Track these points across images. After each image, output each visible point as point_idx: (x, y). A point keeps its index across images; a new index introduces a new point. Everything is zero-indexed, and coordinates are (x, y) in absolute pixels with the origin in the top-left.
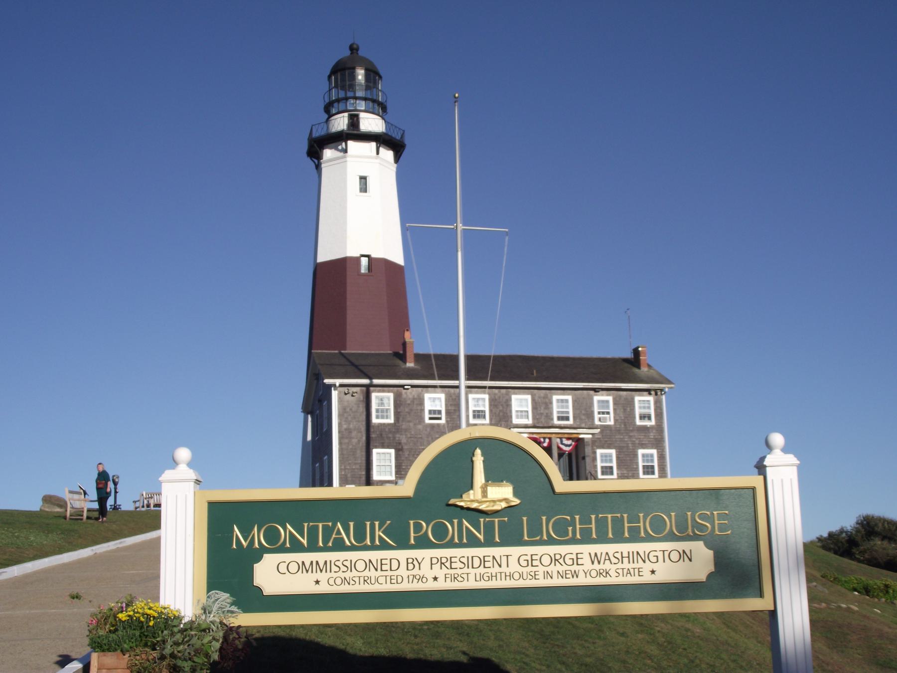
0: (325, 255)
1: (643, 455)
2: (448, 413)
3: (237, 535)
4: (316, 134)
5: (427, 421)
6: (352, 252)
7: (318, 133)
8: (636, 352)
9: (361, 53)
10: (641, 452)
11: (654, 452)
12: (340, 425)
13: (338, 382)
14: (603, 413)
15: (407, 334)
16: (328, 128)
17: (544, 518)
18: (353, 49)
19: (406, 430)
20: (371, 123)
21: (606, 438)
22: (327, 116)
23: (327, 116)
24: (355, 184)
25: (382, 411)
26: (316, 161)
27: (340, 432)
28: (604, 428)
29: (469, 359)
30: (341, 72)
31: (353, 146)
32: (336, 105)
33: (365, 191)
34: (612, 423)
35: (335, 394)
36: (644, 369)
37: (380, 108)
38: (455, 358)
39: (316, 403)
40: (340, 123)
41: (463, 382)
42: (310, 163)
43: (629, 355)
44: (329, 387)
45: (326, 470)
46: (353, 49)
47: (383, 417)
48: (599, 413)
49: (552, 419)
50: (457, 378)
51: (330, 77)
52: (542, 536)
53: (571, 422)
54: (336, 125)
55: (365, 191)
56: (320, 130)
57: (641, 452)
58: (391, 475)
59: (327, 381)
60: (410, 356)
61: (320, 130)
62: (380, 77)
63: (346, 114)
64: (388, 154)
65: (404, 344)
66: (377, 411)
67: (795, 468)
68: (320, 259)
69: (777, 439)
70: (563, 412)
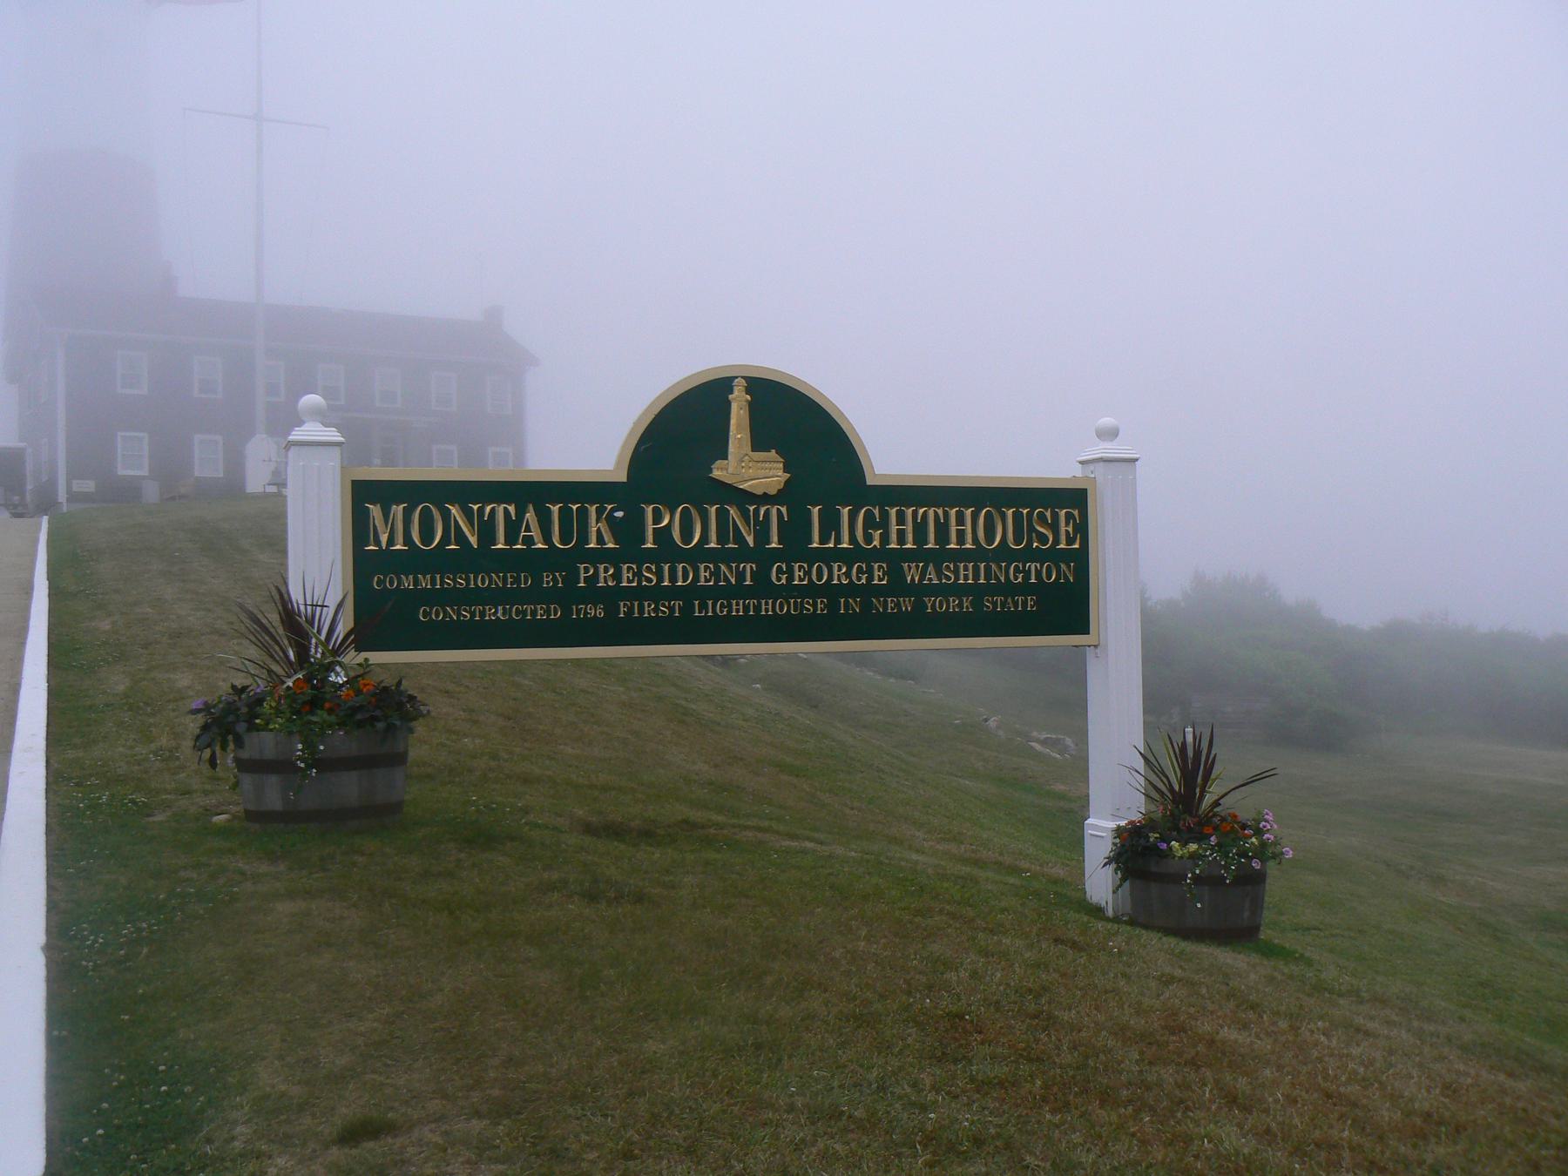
3: (472, 525)
52: (838, 541)
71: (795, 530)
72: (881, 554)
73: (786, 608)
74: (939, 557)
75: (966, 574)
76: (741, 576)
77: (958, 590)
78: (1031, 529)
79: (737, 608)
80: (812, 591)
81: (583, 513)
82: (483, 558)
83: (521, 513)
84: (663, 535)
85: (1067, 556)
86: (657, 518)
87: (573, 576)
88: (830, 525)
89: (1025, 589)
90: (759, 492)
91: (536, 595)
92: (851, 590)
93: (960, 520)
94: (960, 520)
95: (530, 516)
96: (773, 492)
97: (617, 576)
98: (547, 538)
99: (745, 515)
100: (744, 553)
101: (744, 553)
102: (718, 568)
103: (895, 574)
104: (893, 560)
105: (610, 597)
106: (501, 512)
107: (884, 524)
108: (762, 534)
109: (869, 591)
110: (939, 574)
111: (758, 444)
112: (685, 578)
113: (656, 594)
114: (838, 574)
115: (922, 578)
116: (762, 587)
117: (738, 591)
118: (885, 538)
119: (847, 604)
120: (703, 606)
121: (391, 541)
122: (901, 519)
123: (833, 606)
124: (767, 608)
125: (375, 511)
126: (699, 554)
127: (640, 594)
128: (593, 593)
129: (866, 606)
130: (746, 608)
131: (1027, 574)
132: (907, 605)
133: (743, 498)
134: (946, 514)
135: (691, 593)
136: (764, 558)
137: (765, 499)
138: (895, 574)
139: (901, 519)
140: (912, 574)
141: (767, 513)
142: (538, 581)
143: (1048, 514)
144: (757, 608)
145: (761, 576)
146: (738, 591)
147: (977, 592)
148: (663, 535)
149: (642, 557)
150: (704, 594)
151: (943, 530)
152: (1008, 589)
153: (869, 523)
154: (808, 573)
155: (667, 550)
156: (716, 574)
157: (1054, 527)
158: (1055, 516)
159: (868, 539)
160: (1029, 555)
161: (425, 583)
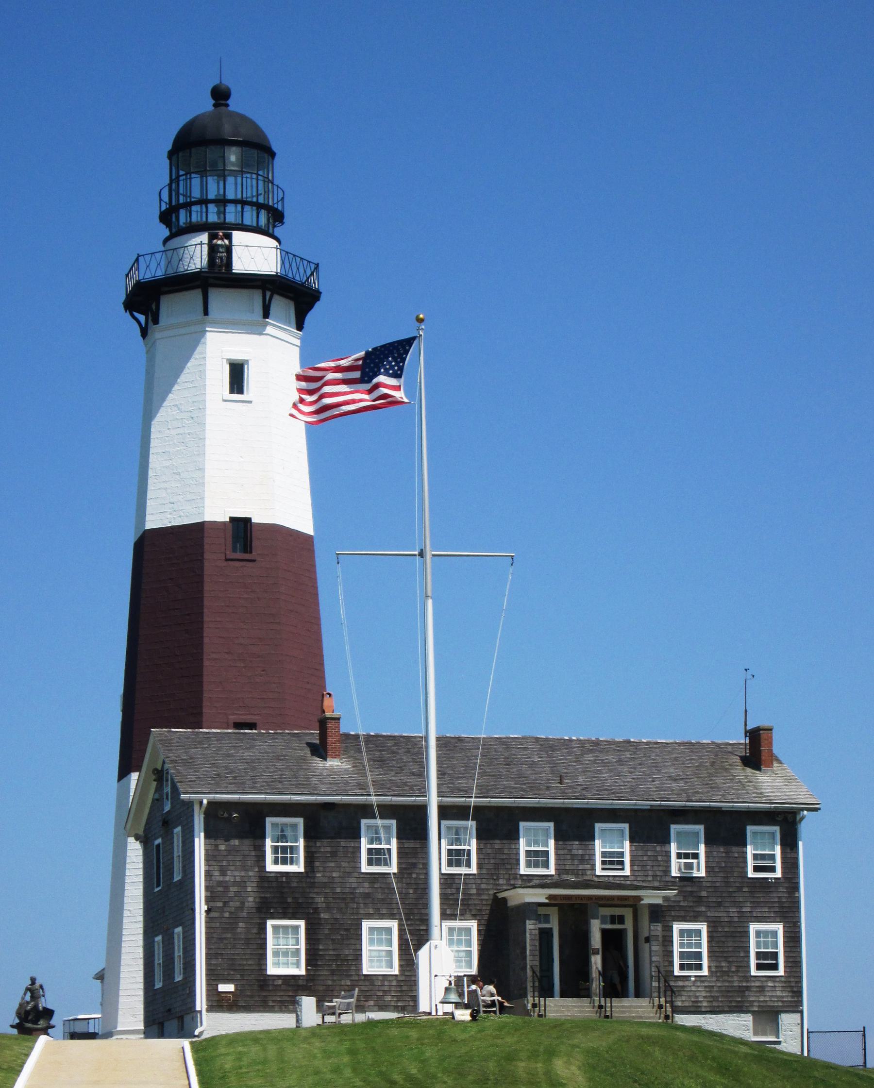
0: (159, 516)
1: (758, 934)
5: (365, 868)
6: (217, 512)
7: (152, 270)
9: (235, 104)
10: (753, 927)
11: (779, 928)
12: (208, 875)
14: (687, 856)
15: (327, 701)
16: (174, 262)
18: (220, 95)
19: (325, 885)
20: (255, 254)
21: (691, 899)
22: (166, 233)
23: (166, 233)
25: (284, 849)
26: (142, 318)
27: (207, 888)
28: (686, 880)
29: (443, 743)
30: (194, 147)
31: (217, 297)
32: (182, 213)
33: (240, 391)
34: (702, 873)
37: (271, 220)
39: (160, 827)
40: (196, 253)
42: (128, 326)
44: (189, 804)
45: (178, 952)
46: (220, 95)
47: (284, 862)
48: (679, 856)
49: (593, 868)
50: (423, 790)
51: (171, 154)
53: (627, 872)
54: (186, 261)
55: (240, 391)
56: (153, 265)
57: (753, 927)
58: (297, 964)
61: (153, 265)
62: (273, 155)
63: (204, 237)
66: (275, 849)
68: (153, 522)
70: (611, 854)
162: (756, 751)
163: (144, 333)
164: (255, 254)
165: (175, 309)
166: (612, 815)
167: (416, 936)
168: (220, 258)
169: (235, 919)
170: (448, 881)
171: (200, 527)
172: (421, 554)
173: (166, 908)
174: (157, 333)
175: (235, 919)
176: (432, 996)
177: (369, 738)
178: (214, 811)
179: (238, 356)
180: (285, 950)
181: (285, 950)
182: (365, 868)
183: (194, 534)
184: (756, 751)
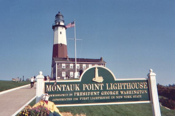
0: (55, 43)
2: (74, 67)
4: (53, 25)
6: (59, 43)
7: (54, 25)
8: (101, 58)
13: (57, 62)
17: (111, 84)
18: (59, 12)
24: (59, 33)
30: (57, 16)
35: (57, 64)
36: (102, 61)
38: (75, 59)
39: (53, 65)
40: (58, 23)
41: (76, 62)
42: (53, 30)
43: (100, 59)
50: (75, 61)
51: (56, 16)
52: (111, 88)
59: (56, 62)
60: (68, 58)
64: (64, 29)
65: (67, 56)
67: (155, 77)
68: (54, 44)
69: (152, 70)
71: (105, 87)
72: (117, 90)
73: (104, 98)
74: (126, 90)
75: (130, 92)
76: (97, 94)
77: (129, 95)
78: (140, 86)
79: (97, 98)
80: (107, 95)
81: (75, 86)
82: (62, 92)
83: (67, 86)
84: (86, 88)
85: (145, 89)
86: (85, 86)
87: (73, 94)
88: (109, 86)
89: (139, 94)
90: (99, 82)
91: (69, 97)
92: (113, 95)
93: (129, 85)
94: (129, 85)
95: (68, 87)
96: (101, 82)
97: (80, 94)
98: (70, 89)
99: (97, 85)
100: (97, 91)
101: (97, 91)
102: (94, 93)
103: (120, 93)
104: (119, 91)
105: (79, 97)
106: (64, 86)
107: (117, 86)
108: (100, 88)
109: (116, 95)
110: (126, 93)
111: (99, 76)
112: (89, 94)
113: (85, 96)
114: (111, 93)
115: (124, 93)
116: (100, 95)
117: (97, 96)
118: (118, 88)
119: (113, 97)
120: (92, 98)
121: (49, 90)
122: (120, 85)
123: (110, 97)
124: (101, 98)
125: (47, 86)
126: (91, 91)
127: (83, 96)
128: (76, 97)
129: (115, 97)
130: (98, 98)
131: (140, 92)
132: (121, 97)
133: (97, 83)
134: (127, 84)
135: (90, 96)
136: (100, 91)
137: (100, 83)
138: (120, 93)
139: (120, 85)
140: (122, 92)
141: (100, 85)
142: (69, 95)
143: (142, 84)
144: (100, 98)
145: (100, 94)
146: (97, 96)
147: (132, 95)
148: (86, 88)
149: (83, 92)
150: (92, 96)
151: (126, 87)
152: (137, 94)
153: (115, 86)
154: (107, 93)
155: (86, 90)
156: (94, 93)
157: (143, 85)
158: (143, 84)
159: (115, 88)
160: (139, 89)
161: (53, 96)
162: (101, 59)
163: (54, 30)
164: (62, 24)
165: (56, 28)
166: (90, 64)
167: (74, 72)
168: (59, 23)
169: (59, 72)
170: (77, 69)
171: (58, 44)
172: (75, 39)
173: (54, 71)
174: (55, 30)
175: (59, 72)
176: (76, 77)
177: (71, 58)
178: (58, 63)
179: (61, 31)
180: (64, 74)
181: (64, 74)
182: (70, 68)
183: (57, 45)
184: (101, 59)
